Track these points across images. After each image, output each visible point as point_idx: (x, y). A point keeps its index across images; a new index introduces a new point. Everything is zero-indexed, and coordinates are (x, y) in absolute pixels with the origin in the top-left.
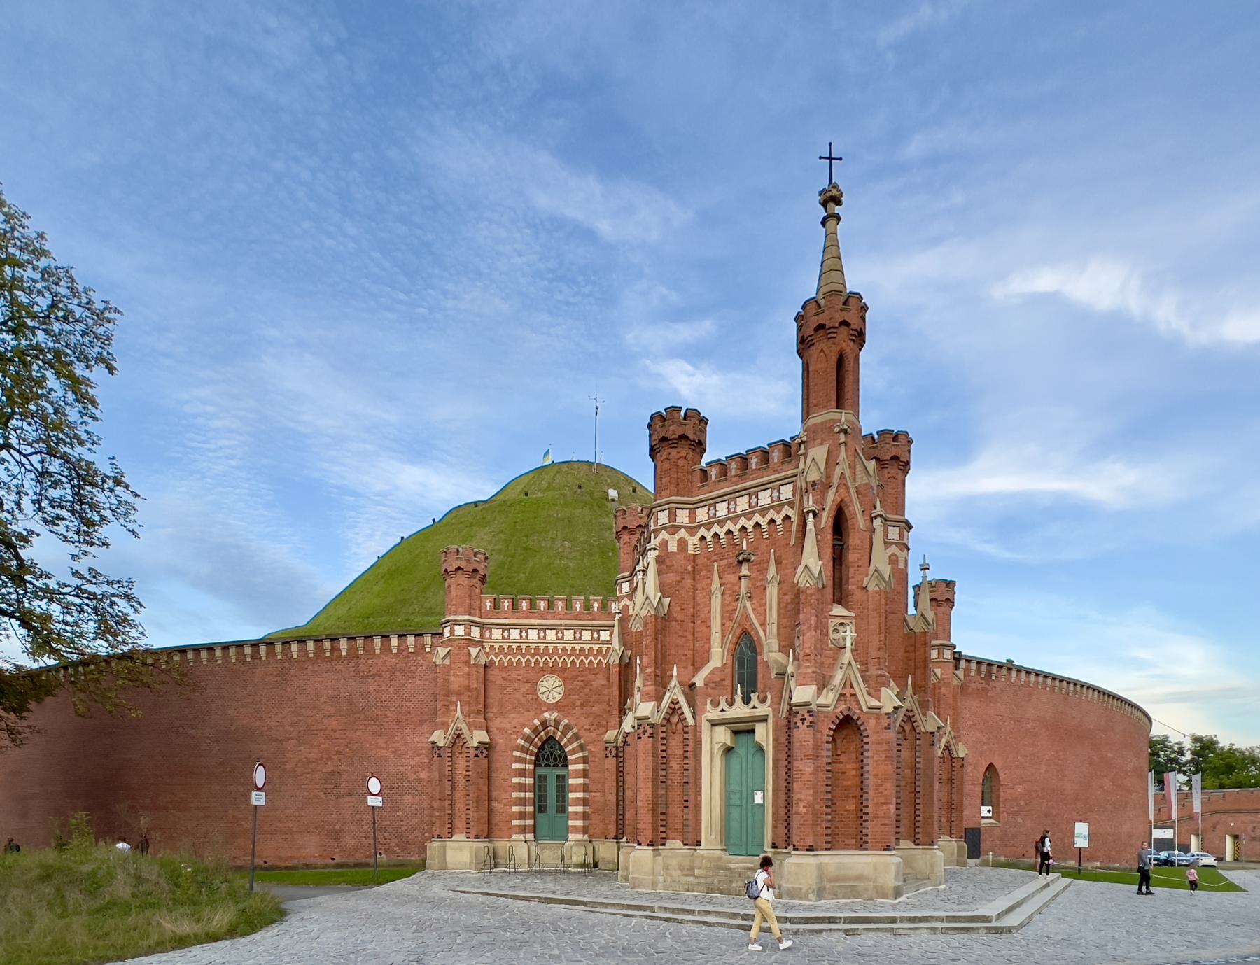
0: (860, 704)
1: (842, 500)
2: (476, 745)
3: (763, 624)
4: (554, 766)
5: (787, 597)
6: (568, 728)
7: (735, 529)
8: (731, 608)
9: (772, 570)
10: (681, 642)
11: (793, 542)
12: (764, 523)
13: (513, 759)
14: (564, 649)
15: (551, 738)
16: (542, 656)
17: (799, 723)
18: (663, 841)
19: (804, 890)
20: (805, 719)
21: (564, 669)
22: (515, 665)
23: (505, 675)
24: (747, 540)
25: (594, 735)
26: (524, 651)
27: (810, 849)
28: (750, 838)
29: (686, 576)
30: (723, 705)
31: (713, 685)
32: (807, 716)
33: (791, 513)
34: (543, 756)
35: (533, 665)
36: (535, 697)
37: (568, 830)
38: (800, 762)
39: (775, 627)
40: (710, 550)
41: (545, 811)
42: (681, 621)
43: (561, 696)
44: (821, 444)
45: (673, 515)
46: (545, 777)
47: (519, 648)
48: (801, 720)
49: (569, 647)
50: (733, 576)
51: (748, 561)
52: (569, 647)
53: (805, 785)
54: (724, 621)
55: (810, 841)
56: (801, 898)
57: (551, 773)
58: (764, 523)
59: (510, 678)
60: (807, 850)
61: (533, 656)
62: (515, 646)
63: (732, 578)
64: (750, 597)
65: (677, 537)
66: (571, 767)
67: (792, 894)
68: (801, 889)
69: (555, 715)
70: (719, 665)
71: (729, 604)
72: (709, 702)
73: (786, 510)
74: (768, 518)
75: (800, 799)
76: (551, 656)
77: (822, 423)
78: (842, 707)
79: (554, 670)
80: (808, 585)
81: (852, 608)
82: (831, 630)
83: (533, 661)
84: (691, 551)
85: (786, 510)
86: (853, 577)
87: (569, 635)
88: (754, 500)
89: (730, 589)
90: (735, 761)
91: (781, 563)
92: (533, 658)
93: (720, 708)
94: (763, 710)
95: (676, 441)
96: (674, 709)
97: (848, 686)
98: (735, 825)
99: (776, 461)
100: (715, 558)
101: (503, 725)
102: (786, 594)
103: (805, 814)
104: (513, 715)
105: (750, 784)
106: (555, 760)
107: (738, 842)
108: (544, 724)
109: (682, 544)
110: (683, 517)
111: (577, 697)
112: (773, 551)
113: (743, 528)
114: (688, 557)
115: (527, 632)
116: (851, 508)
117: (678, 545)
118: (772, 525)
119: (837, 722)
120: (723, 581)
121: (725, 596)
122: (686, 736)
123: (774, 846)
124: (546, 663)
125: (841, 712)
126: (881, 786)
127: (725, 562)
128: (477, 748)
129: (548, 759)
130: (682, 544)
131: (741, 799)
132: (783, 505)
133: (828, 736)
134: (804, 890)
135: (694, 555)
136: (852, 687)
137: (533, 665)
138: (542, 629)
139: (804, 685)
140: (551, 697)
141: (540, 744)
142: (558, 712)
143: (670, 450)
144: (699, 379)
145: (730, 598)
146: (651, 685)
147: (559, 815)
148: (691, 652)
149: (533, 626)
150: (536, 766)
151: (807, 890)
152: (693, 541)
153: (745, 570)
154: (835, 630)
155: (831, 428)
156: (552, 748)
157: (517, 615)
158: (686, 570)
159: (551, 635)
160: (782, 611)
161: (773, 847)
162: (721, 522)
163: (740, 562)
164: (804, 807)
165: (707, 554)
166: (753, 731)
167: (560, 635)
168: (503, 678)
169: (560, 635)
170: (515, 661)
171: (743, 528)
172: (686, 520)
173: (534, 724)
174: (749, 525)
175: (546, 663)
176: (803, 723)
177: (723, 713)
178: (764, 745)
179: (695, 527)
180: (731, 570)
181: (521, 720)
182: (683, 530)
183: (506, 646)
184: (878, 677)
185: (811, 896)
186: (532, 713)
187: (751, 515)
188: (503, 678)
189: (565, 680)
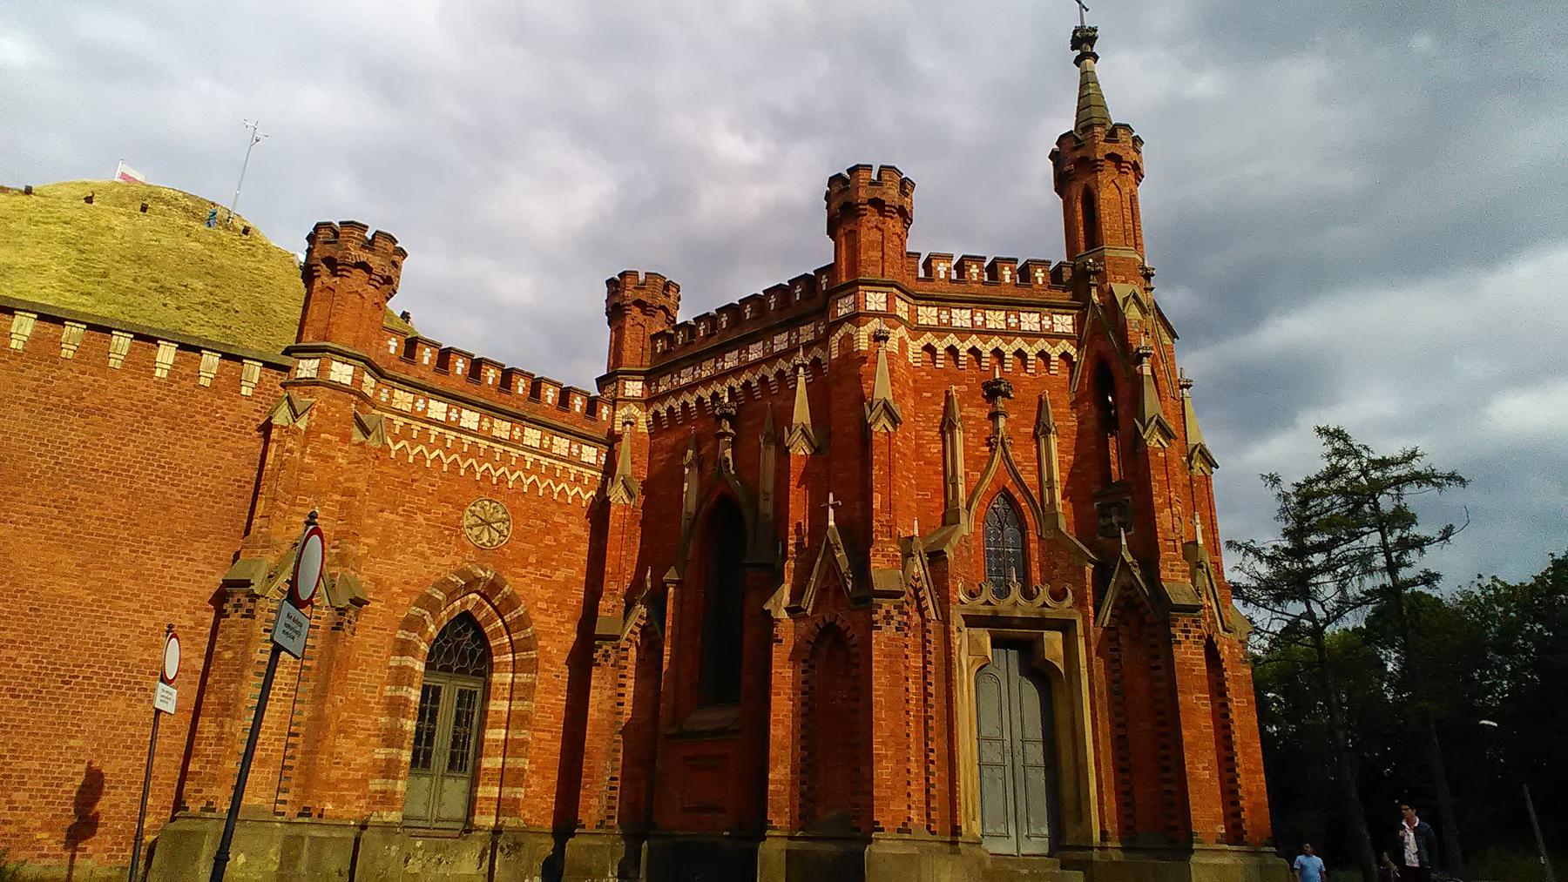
7: (986, 350)
14: (521, 459)
20: (1189, 632)
33: (1072, 351)
35: (462, 472)
47: (442, 438)
48: (1182, 631)
61: (465, 457)
92: (464, 462)
93: (982, 599)
124: (486, 476)
137: (462, 472)
176: (1187, 637)
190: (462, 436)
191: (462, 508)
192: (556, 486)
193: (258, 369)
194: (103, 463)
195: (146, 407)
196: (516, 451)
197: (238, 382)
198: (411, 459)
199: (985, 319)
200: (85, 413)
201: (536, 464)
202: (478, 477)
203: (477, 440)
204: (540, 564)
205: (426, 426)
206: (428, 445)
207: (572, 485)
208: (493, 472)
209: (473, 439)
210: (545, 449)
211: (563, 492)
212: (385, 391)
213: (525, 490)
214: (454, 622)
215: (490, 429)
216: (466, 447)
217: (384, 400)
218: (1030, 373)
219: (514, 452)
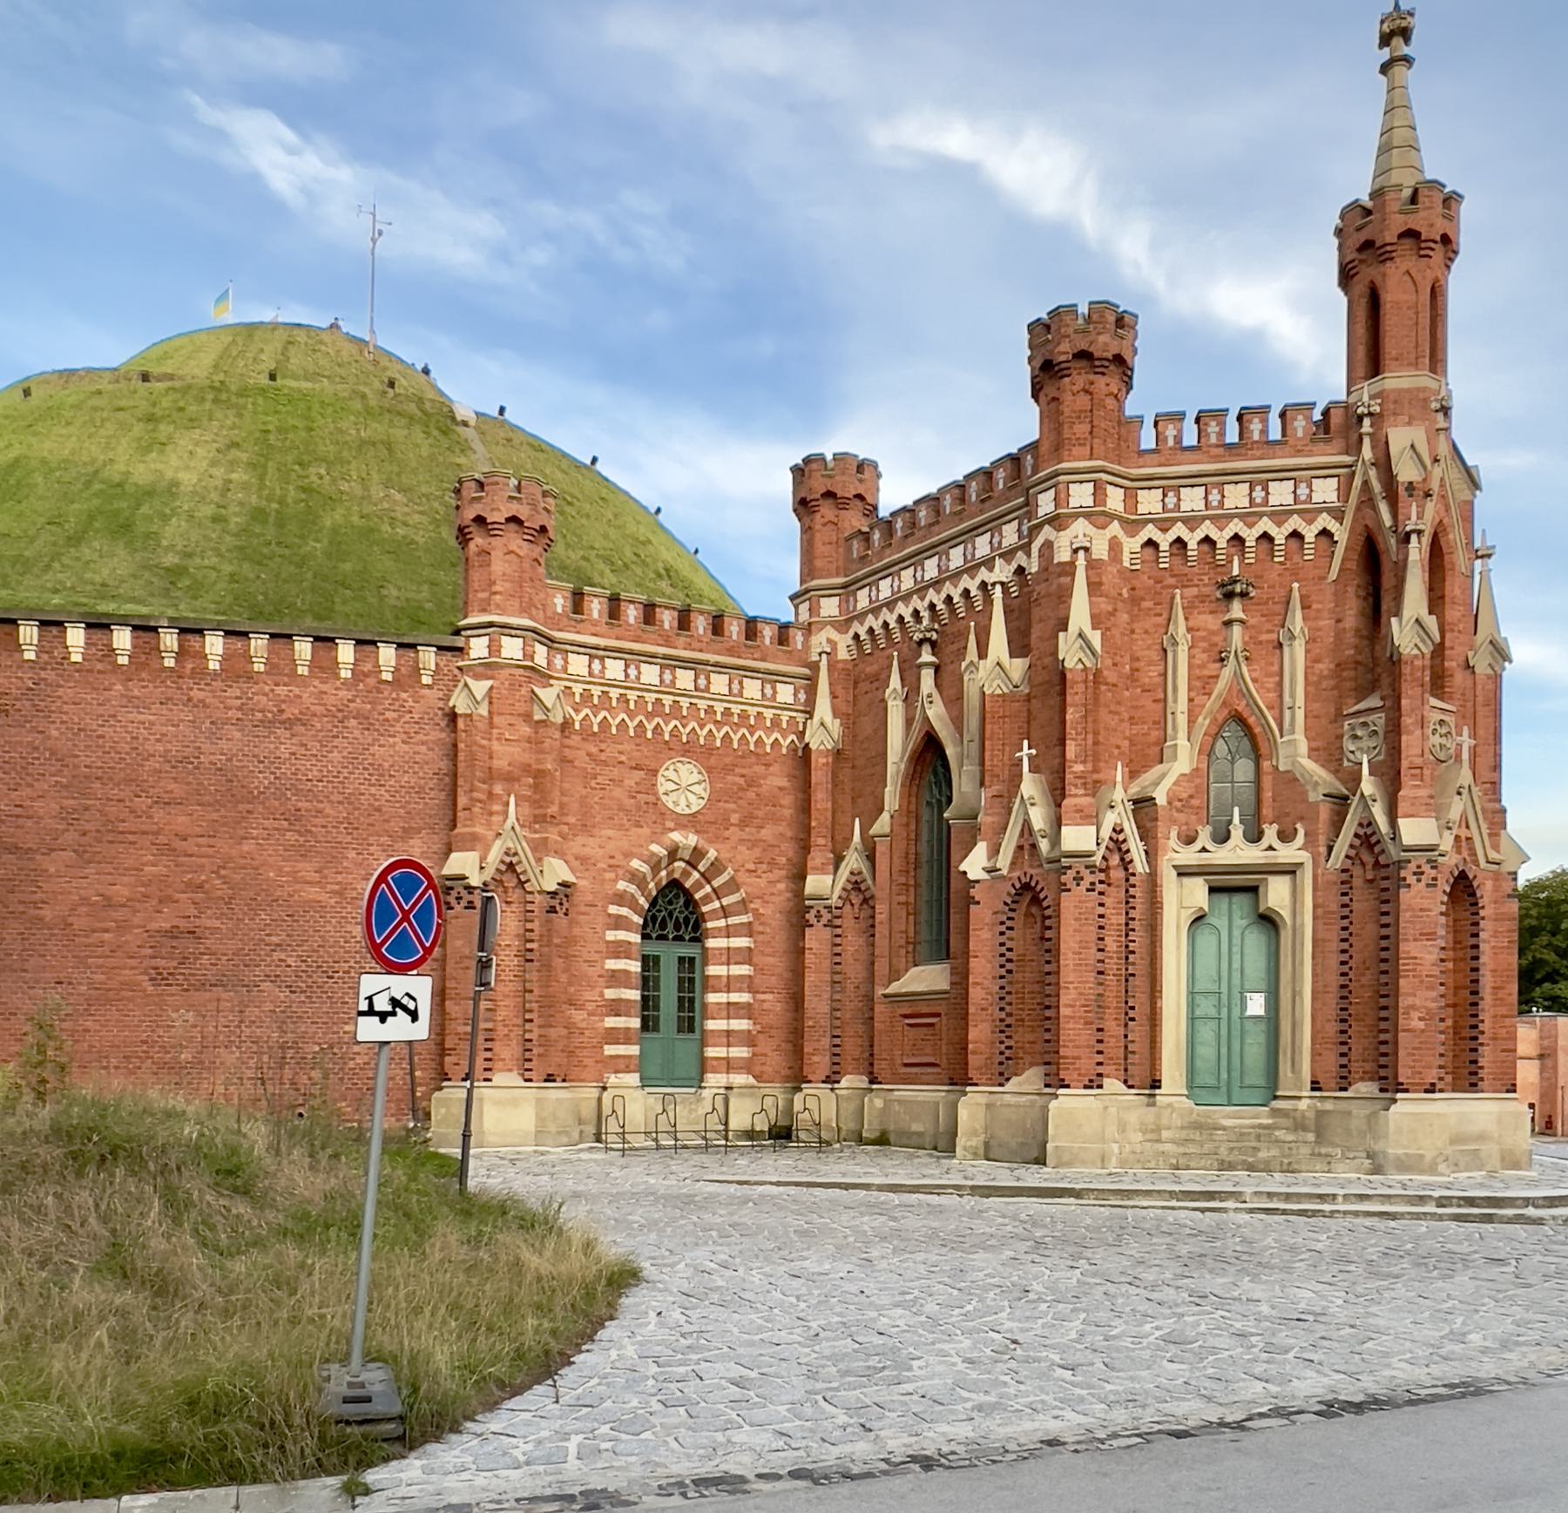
0: (1475, 855)
2: (553, 887)
3: (1278, 707)
4: (675, 939)
5: (1320, 666)
7: (1222, 538)
8: (1206, 672)
9: (1297, 621)
10: (1112, 721)
11: (1333, 575)
12: (1279, 535)
13: (611, 921)
14: (710, 710)
15: (675, 884)
16: (667, 718)
17: (1411, 879)
19: (1428, 1159)
21: (709, 750)
22: (614, 731)
23: (594, 750)
24: (1241, 562)
26: (632, 706)
27: (1431, 1089)
28: (1236, 1074)
29: (1120, 605)
30: (1204, 838)
31: (1179, 804)
32: (1426, 868)
35: (649, 735)
36: (651, 799)
37: (703, 1066)
38: (1413, 944)
39: (1300, 715)
40: (1161, 566)
41: (656, 1029)
42: (1115, 685)
43: (703, 803)
44: (1409, 423)
45: (1131, 497)
46: (656, 959)
47: (623, 699)
49: (719, 708)
50: (1210, 618)
51: (1244, 595)
52: (719, 708)
53: (1422, 982)
54: (1193, 694)
55: (1432, 1076)
56: (1422, 1172)
57: (669, 953)
58: (1310, 534)
59: (603, 757)
60: (1426, 1091)
61: (650, 716)
62: (614, 693)
63: (1212, 622)
66: (711, 943)
67: (1406, 1165)
68: (1422, 1156)
69: (692, 840)
70: (1187, 771)
72: (1174, 834)
73: (1325, 521)
74: (1288, 527)
75: (1413, 1007)
77: (1408, 391)
79: (688, 750)
80: (1416, 652)
81: (1451, 698)
83: (650, 727)
85: (1325, 521)
86: (1452, 648)
87: (719, 683)
88: (1259, 494)
89: (1203, 639)
90: (1206, 940)
91: (1309, 607)
94: (1288, 853)
95: (1107, 364)
96: (1118, 844)
98: (1206, 1052)
99: (1300, 434)
100: (1172, 581)
101: (587, 851)
102: (1317, 661)
103: (1423, 1031)
104: (610, 833)
105: (1236, 981)
106: (677, 927)
107: (1211, 1081)
108: (673, 854)
110: (1115, 500)
111: (732, 806)
114: (1122, 572)
115: (638, 668)
116: (1451, 536)
117: (1111, 548)
120: (1191, 624)
121: (1196, 651)
123: (1316, 1086)
124: (675, 733)
126: (1502, 988)
127: (1194, 591)
128: (554, 894)
129: (663, 926)
130: (1115, 546)
131: (1219, 1007)
132: (1320, 511)
134: (1428, 1159)
136: (1468, 827)
137: (649, 735)
138: (668, 666)
139: (1412, 816)
140: (673, 796)
142: (697, 832)
143: (1092, 377)
144: (312, 164)
145: (1204, 656)
146: (1085, 795)
147: (681, 1036)
149: (651, 657)
150: (645, 937)
151: (1435, 1158)
153: (1237, 610)
155: (1426, 400)
157: (616, 630)
158: (1120, 594)
159: (685, 679)
160: (1311, 689)
161: (1313, 1089)
162: (1192, 522)
163: (1229, 596)
164: (1420, 1019)
165: (1153, 574)
167: (702, 682)
168: (589, 754)
169: (702, 682)
170: (614, 722)
171: (1237, 539)
172: (1120, 508)
173: (653, 854)
177: (1205, 855)
179: (1134, 521)
180: (1207, 607)
181: (624, 844)
183: (596, 691)
184: (1493, 812)
185: (1442, 1167)
186: (646, 831)
188: (589, 754)
189: (709, 770)
191: (655, 772)
192: (752, 736)
193: (433, 655)
194: (315, 773)
195: (339, 711)
197: (416, 672)
198: (596, 729)
199: (1223, 496)
200: (289, 724)
202: (667, 737)
205: (606, 689)
206: (610, 709)
212: (559, 656)
214: (662, 891)
215: (673, 682)
217: (559, 667)
218: (1280, 563)
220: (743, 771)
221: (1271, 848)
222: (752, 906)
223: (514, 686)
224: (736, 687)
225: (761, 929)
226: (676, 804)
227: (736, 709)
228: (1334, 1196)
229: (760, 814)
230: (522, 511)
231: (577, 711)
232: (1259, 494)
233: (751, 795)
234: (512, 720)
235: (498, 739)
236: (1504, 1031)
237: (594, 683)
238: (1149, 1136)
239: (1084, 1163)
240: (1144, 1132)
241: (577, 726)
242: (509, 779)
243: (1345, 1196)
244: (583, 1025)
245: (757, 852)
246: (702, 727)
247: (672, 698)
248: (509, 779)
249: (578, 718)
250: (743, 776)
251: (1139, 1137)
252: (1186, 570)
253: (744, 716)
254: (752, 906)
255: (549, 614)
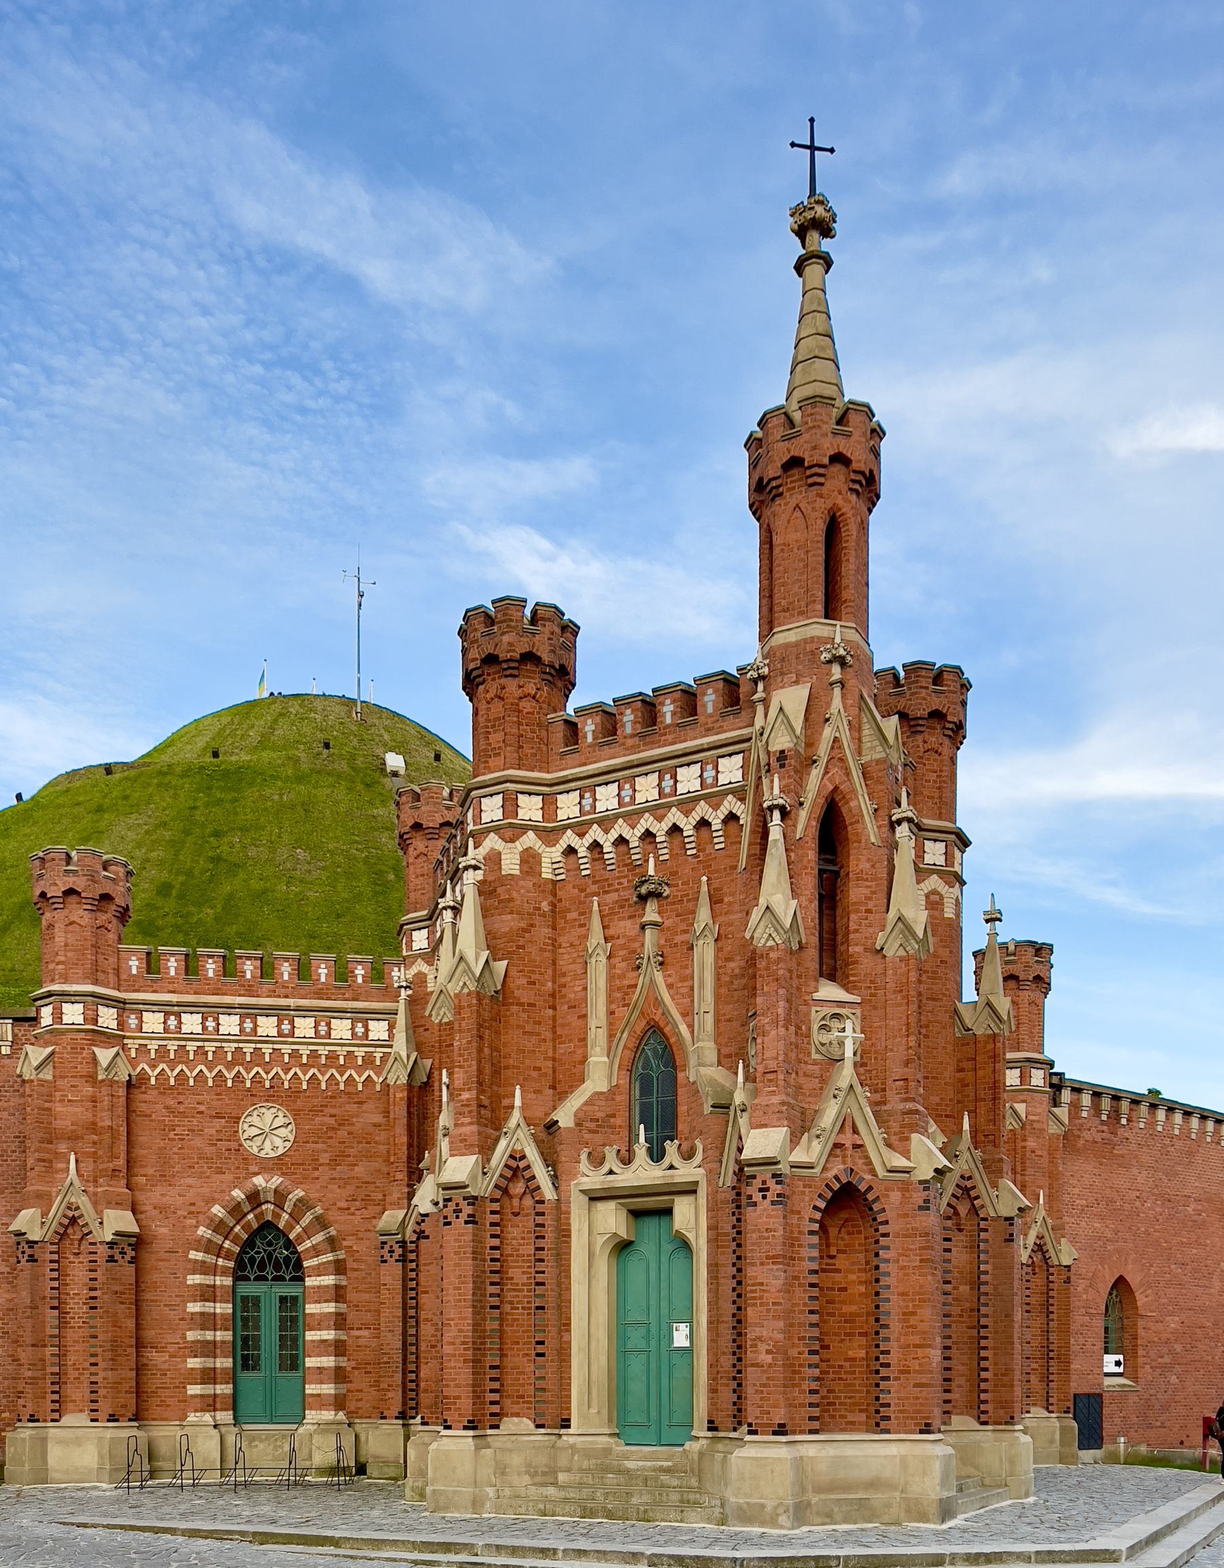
0: (870, 1163)
1: (836, 788)
3: (687, 1013)
4: (275, 1279)
5: (732, 965)
6: (303, 1205)
7: (633, 836)
8: (626, 982)
9: (704, 914)
10: (529, 1043)
11: (743, 863)
13: (190, 1266)
14: (295, 1054)
15: (268, 1226)
17: (757, 1197)
18: (495, 1420)
19: (769, 1509)
20: (767, 1189)
22: (191, 1083)
23: (171, 1102)
24: (656, 858)
25: (357, 1219)
26: (210, 1057)
27: (781, 1430)
28: (665, 1413)
29: (537, 920)
30: (612, 1162)
31: (592, 1125)
32: (771, 1183)
33: (739, 809)
34: (252, 1260)
35: (230, 1084)
36: (234, 1145)
37: (305, 1402)
38: (759, 1268)
39: (709, 1019)
40: (584, 873)
41: (256, 1367)
42: (530, 1005)
46: (256, 1301)
47: (201, 1051)
48: (761, 1190)
49: (305, 1051)
50: (629, 923)
51: (658, 895)
52: (305, 1051)
53: (768, 1311)
54: (613, 1006)
55: (779, 1417)
56: (763, 1524)
57: (268, 1293)
59: (182, 1108)
60: (775, 1433)
62: (191, 1047)
63: (626, 927)
64: (661, 964)
65: (519, 846)
66: (309, 1282)
67: (748, 1515)
68: (763, 1506)
69: (276, 1181)
70: (604, 1088)
71: (622, 976)
72: (584, 1157)
73: (730, 804)
74: (696, 816)
75: (760, 1339)
76: (267, 1067)
77: (797, 644)
78: (837, 1168)
79: (274, 1095)
80: (770, 943)
81: (855, 988)
82: (815, 1027)
84: (547, 873)
85: (730, 804)
86: (856, 931)
87: (304, 1027)
88: (668, 782)
89: (623, 947)
91: (721, 901)
93: (606, 1169)
94: (688, 1172)
97: (848, 1130)
98: (637, 1387)
99: (710, 709)
100: (594, 888)
101: (167, 1200)
102: (728, 959)
103: (770, 1365)
104: (189, 1181)
105: (664, 1311)
106: (277, 1267)
107: (641, 1419)
108: (254, 1198)
109: (530, 860)
110: (530, 808)
111: (320, 1146)
112: (704, 878)
113: (648, 835)
116: (852, 804)
117: (523, 861)
118: (704, 830)
119: (829, 1195)
120: (611, 932)
121: (615, 960)
122: (539, 1220)
123: (712, 1427)
124: (257, 1079)
125: (836, 1178)
126: (913, 1314)
127: (613, 897)
129: (262, 1267)
130: (530, 860)
131: (647, 1337)
132: (725, 793)
133: (811, 1220)
134: (769, 1509)
135: (554, 883)
137: (230, 1084)
139: (765, 1126)
141: (245, 1236)
145: (624, 965)
146: (471, 1123)
147: (284, 1374)
148: (550, 1064)
149: (229, 1009)
150: (237, 1279)
151: (776, 1508)
152: (551, 856)
153: (651, 913)
154: (823, 1027)
155: (814, 654)
156: (270, 1244)
157: (195, 986)
158: (539, 909)
159: (267, 1026)
160: (723, 991)
161: (710, 1429)
162: (605, 823)
163: (643, 899)
164: (768, 1352)
165: (578, 882)
166: (668, 1212)
167: (286, 1027)
168: (167, 1107)
171: (648, 835)
172: (538, 816)
174: (660, 829)
175: (257, 1079)
176: (764, 1197)
177: (611, 1177)
178: (691, 1236)
179: (553, 830)
180: (626, 912)
181: (205, 1190)
182: (531, 834)
183: (172, 1046)
184: (904, 1113)
185: (783, 1519)
186: (228, 1177)
187: (661, 811)
188: (167, 1107)
189: (296, 1114)
190: (223, 1045)
196: (288, 1046)
198: (172, 1082)
201: (314, 1055)
202: (248, 1084)
203: (241, 1045)
204: (334, 1163)
205: (183, 1043)
206: (187, 1063)
207: (360, 1070)
208: (264, 1075)
209: (236, 1045)
210: (360, 1020)
211: (350, 1079)
212: (133, 1016)
213: (305, 1087)
216: (229, 1055)
219: (286, 1049)
220: (333, 1111)
221: (671, 1167)
222: (345, 1243)
223: (75, 1049)
224: (323, 1029)
225: (355, 1265)
226: (274, 1148)
227: (324, 1051)
228: (555, 1551)
229: (352, 1152)
230: (79, 883)
231: (153, 1067)
232: (668, 782)
233: (343, 1133)
234: (74, 1082)
235: (61, 1101)
236: (917, 1362)
237: (170, 1039)
238: (538, 1479)
239: (457, 1508)
240: (532, 1476)
241: (153, 1081)
242: (73, 1137)
243: (564, 1551)
244: (166, 1366)
245: (350, 1190)
246: (286, 1071)
247: (253, 1045)
248: (73, 1137)
249: (153, 1074)
250: (334, 1116)
251: (526, 1479)
252: (607, 875)
253: (332, 1057)
254: (345, 1243)
255: (124, 976)
